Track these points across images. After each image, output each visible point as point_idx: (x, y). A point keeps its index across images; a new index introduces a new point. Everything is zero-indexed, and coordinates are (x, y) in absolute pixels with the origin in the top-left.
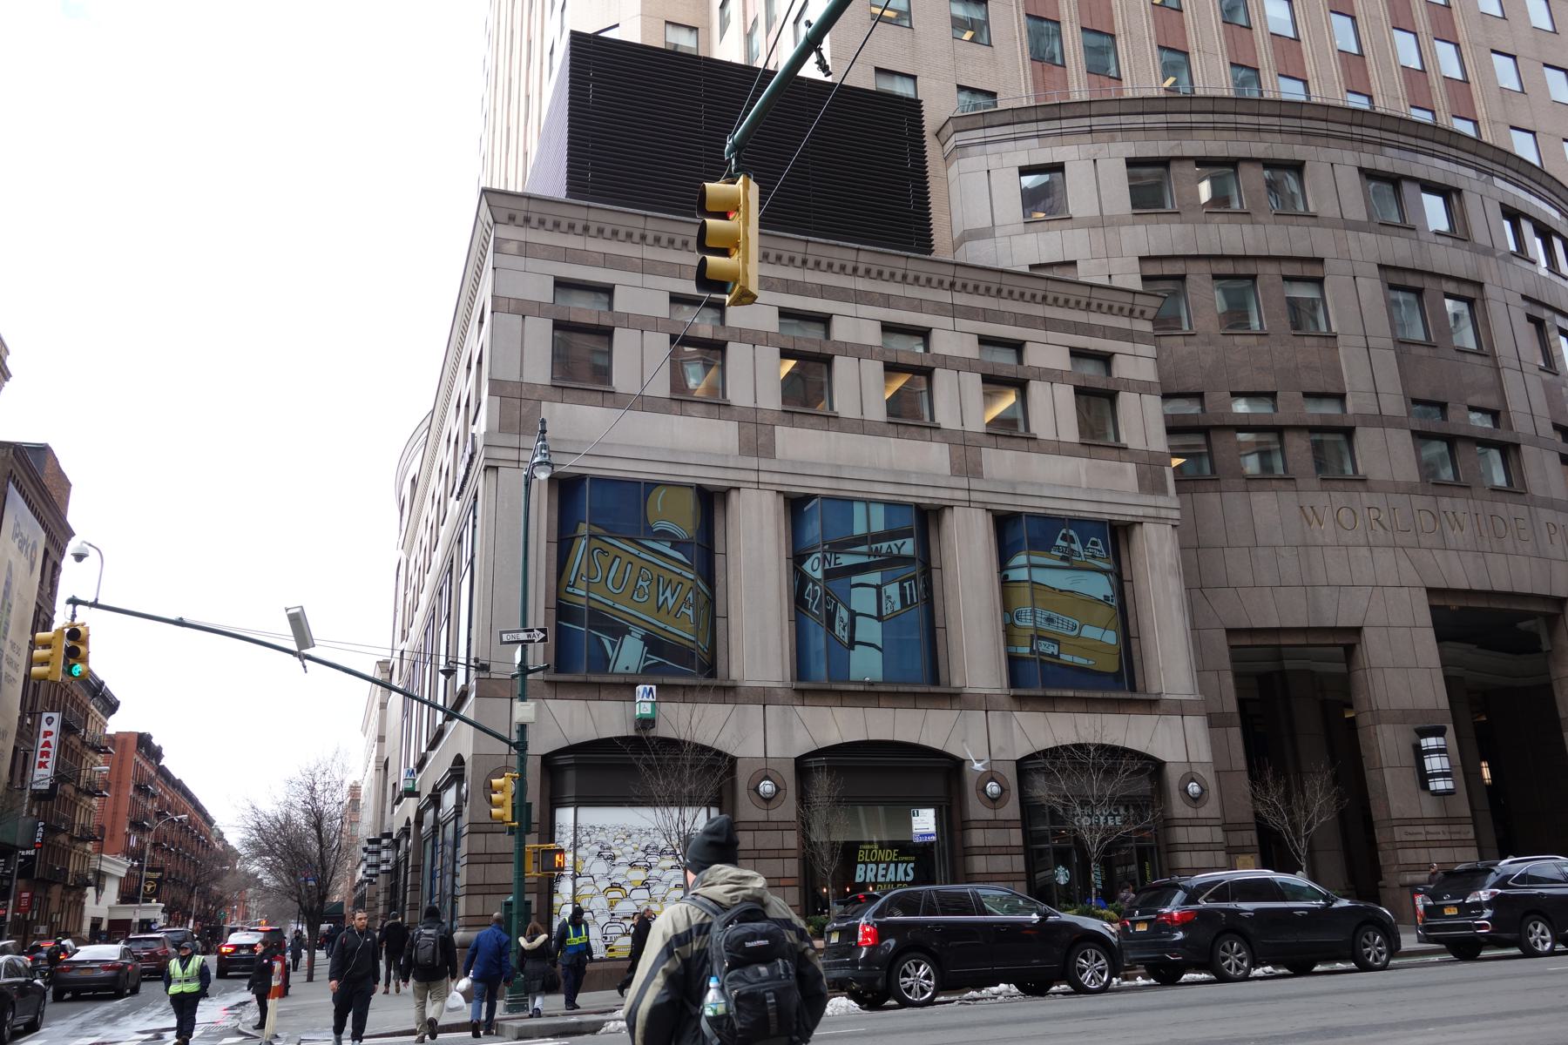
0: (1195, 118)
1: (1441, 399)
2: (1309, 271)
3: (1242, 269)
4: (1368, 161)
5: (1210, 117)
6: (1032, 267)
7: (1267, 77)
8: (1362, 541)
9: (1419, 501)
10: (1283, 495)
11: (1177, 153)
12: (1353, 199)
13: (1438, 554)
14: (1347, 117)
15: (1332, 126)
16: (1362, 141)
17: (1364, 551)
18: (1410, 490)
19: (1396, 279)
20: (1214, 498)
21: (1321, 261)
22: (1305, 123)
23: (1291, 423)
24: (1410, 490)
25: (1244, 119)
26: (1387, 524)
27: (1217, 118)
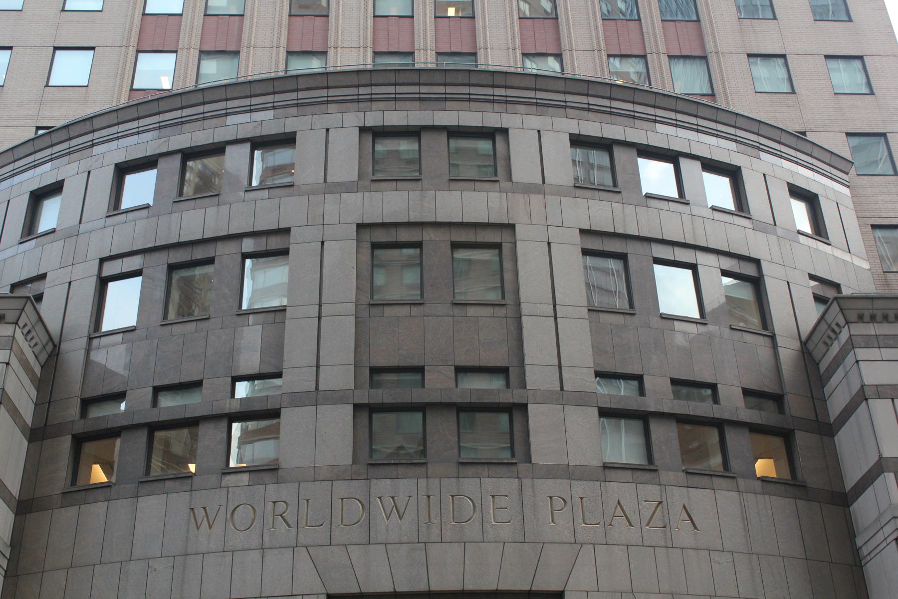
0: (186, 112)
1: (415, 362)
2: (274, 243)
3: (199, 253)
4: (373, 119)
5: (200, 109)
6: (14, 287)
7: (659, 62)
8: (256, 543)
9: (356, 487)
10: (173, 497)
11: (164, 150)
12: (561, 163)
13: (355, 552)
14: (354, 80)
15: (332, 92)
16: (371, 100)
17: (256, 555)
18: (337, 475)
19: (381, 236)
20: (100, 508)
21: (287, 231)
22: (301, 95)
23: (205, 413)
24: (337, 475)
25: (236, 103)
26: (292, 520)
27: (208, 108)
